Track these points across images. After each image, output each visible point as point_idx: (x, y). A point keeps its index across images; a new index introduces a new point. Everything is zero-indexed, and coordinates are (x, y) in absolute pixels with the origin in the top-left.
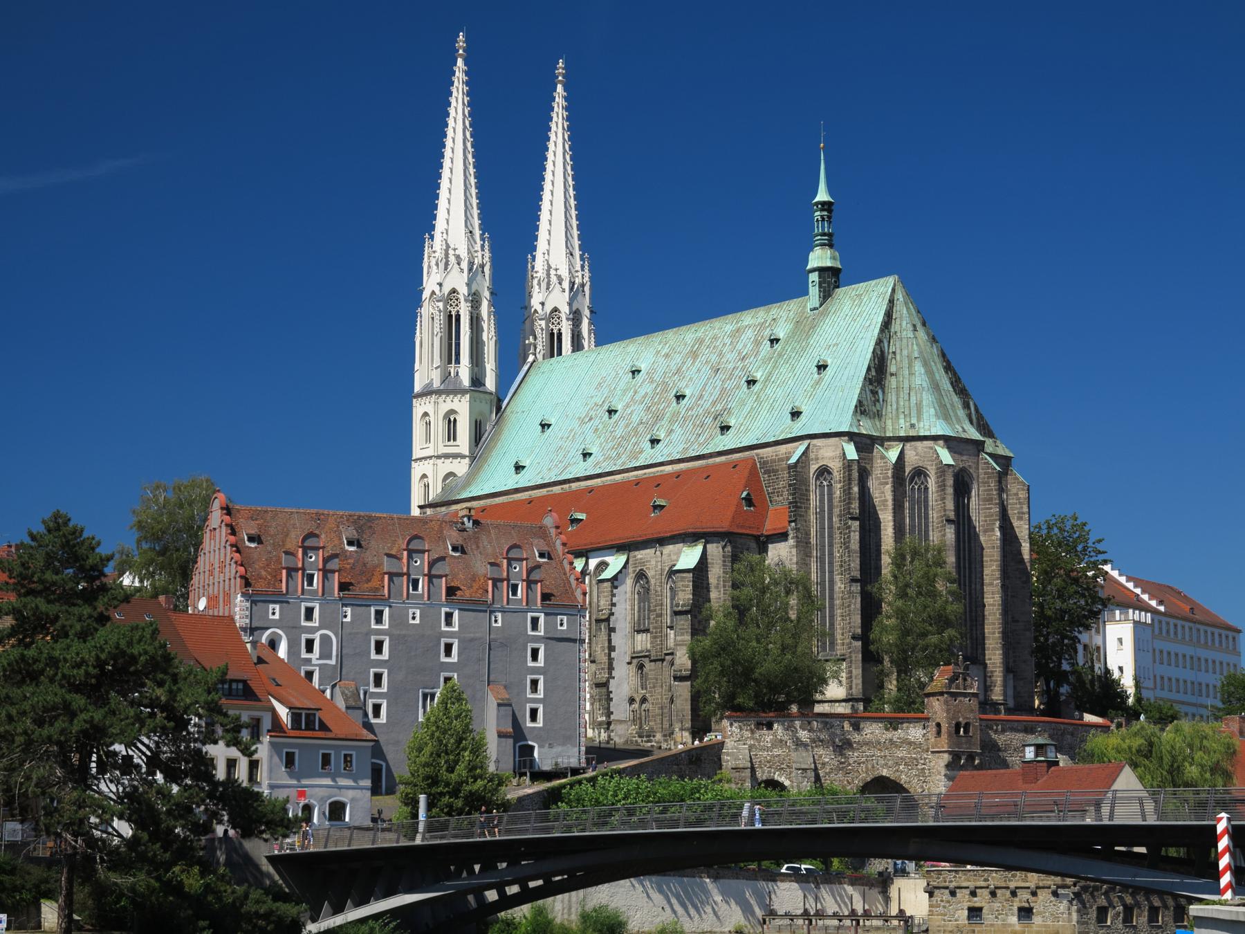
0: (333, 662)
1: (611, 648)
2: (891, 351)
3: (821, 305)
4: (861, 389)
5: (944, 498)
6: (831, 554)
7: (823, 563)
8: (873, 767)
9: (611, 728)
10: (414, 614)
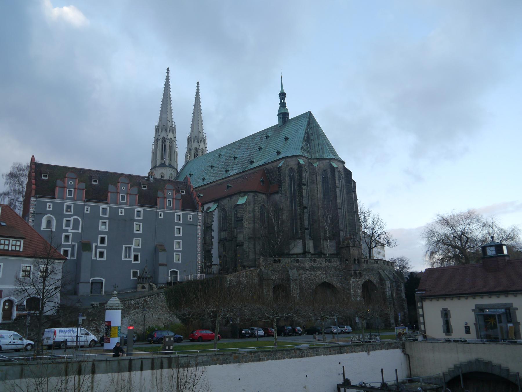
0: (80, 231)
1: (213, 237)
3: (283, 125)
4: (303, 142)
5: (335, 179)
6: (295, 200)
8: (321, 277)
9: (212, 267)
10: (122, 211)
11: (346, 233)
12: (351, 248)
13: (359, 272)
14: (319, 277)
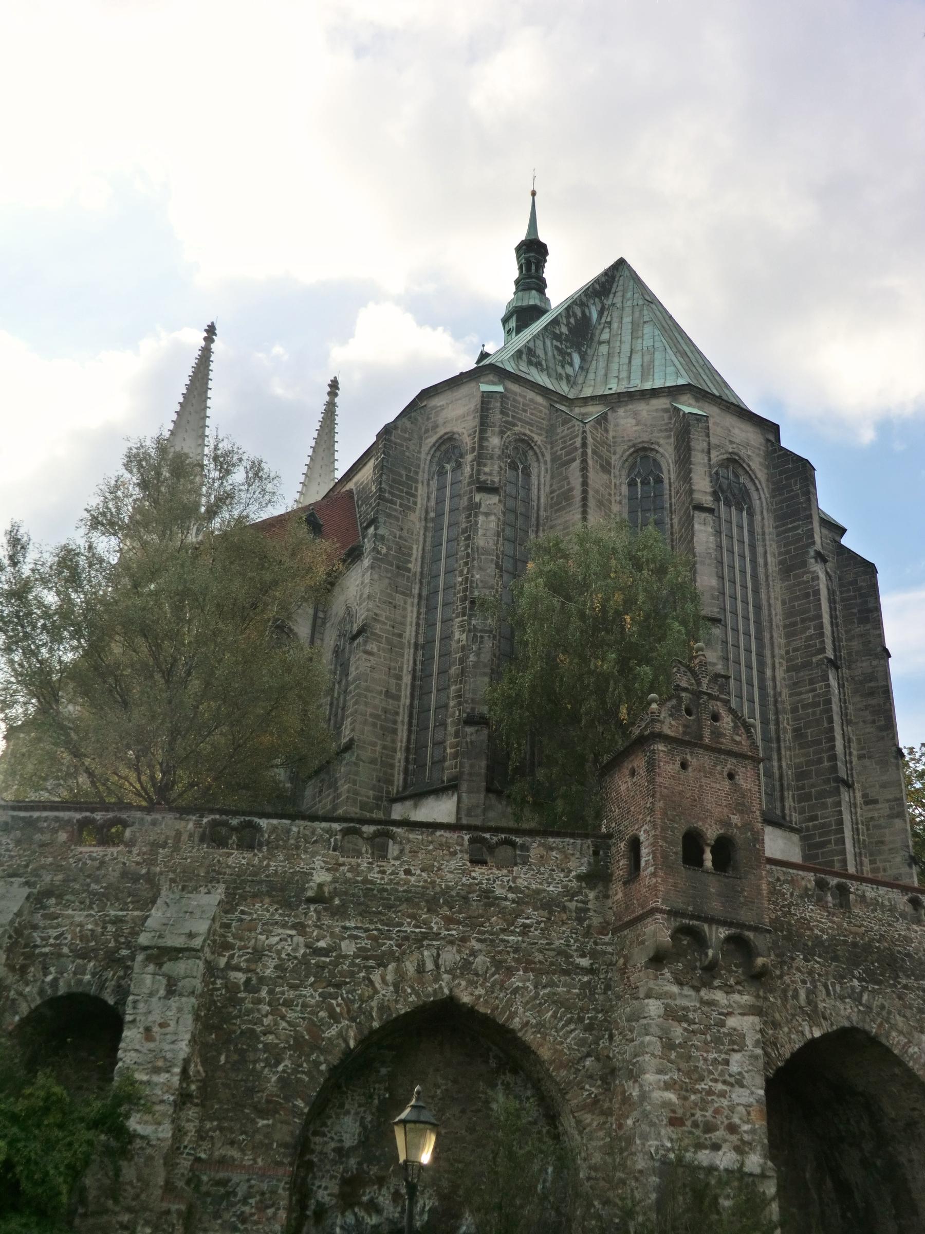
2: (603, 320)
5: (690, 471)
7: (431, 609)
8: (421, 969)
11: (777, 784)
12: (661, 747)
13: (728, 939)
14: (398, 960)
